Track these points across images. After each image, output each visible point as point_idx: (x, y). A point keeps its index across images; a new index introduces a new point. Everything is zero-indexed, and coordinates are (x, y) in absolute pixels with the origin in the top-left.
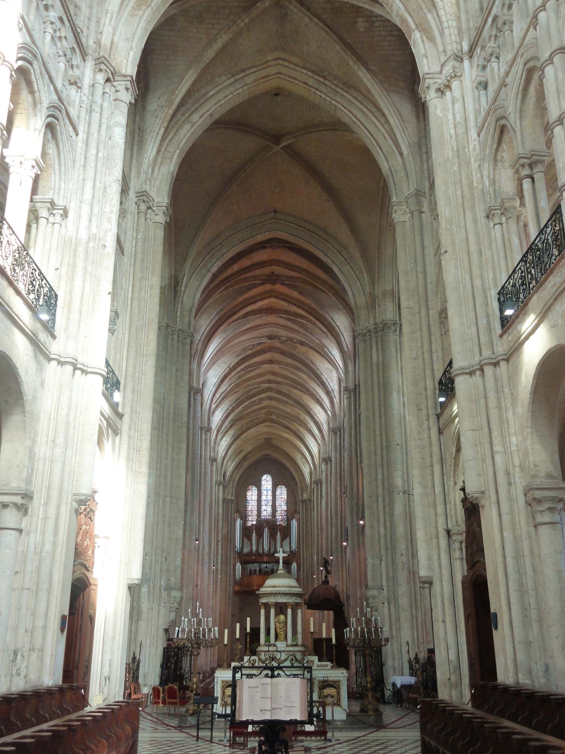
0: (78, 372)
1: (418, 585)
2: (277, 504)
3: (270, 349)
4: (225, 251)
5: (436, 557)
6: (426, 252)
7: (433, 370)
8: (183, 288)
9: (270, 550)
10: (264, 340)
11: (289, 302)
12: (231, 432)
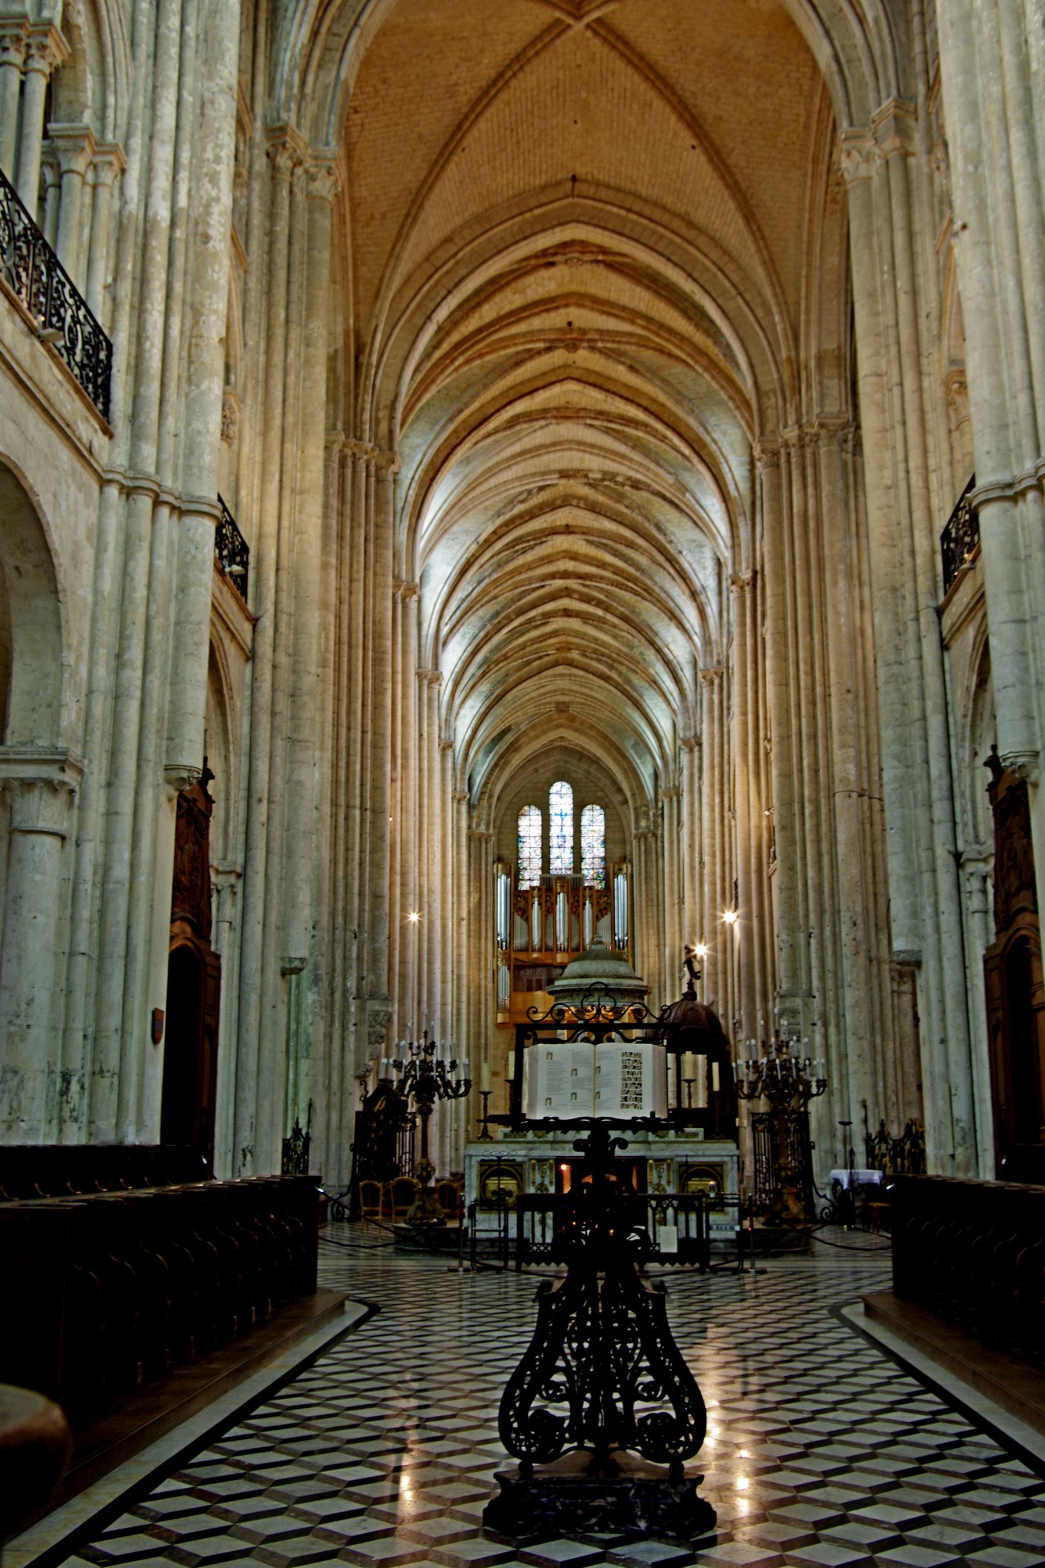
0: (164, 511)
1: (888, 986)
2: (584, 844)
3: (567, 501)
4: (464, 272)
5: (929, 910)
6: (918, 248)
7: (929, 510)
8: (374, 359)
9: (569, 939)
10: (553, 479)
11: (608, 391)
12: (484, 687)
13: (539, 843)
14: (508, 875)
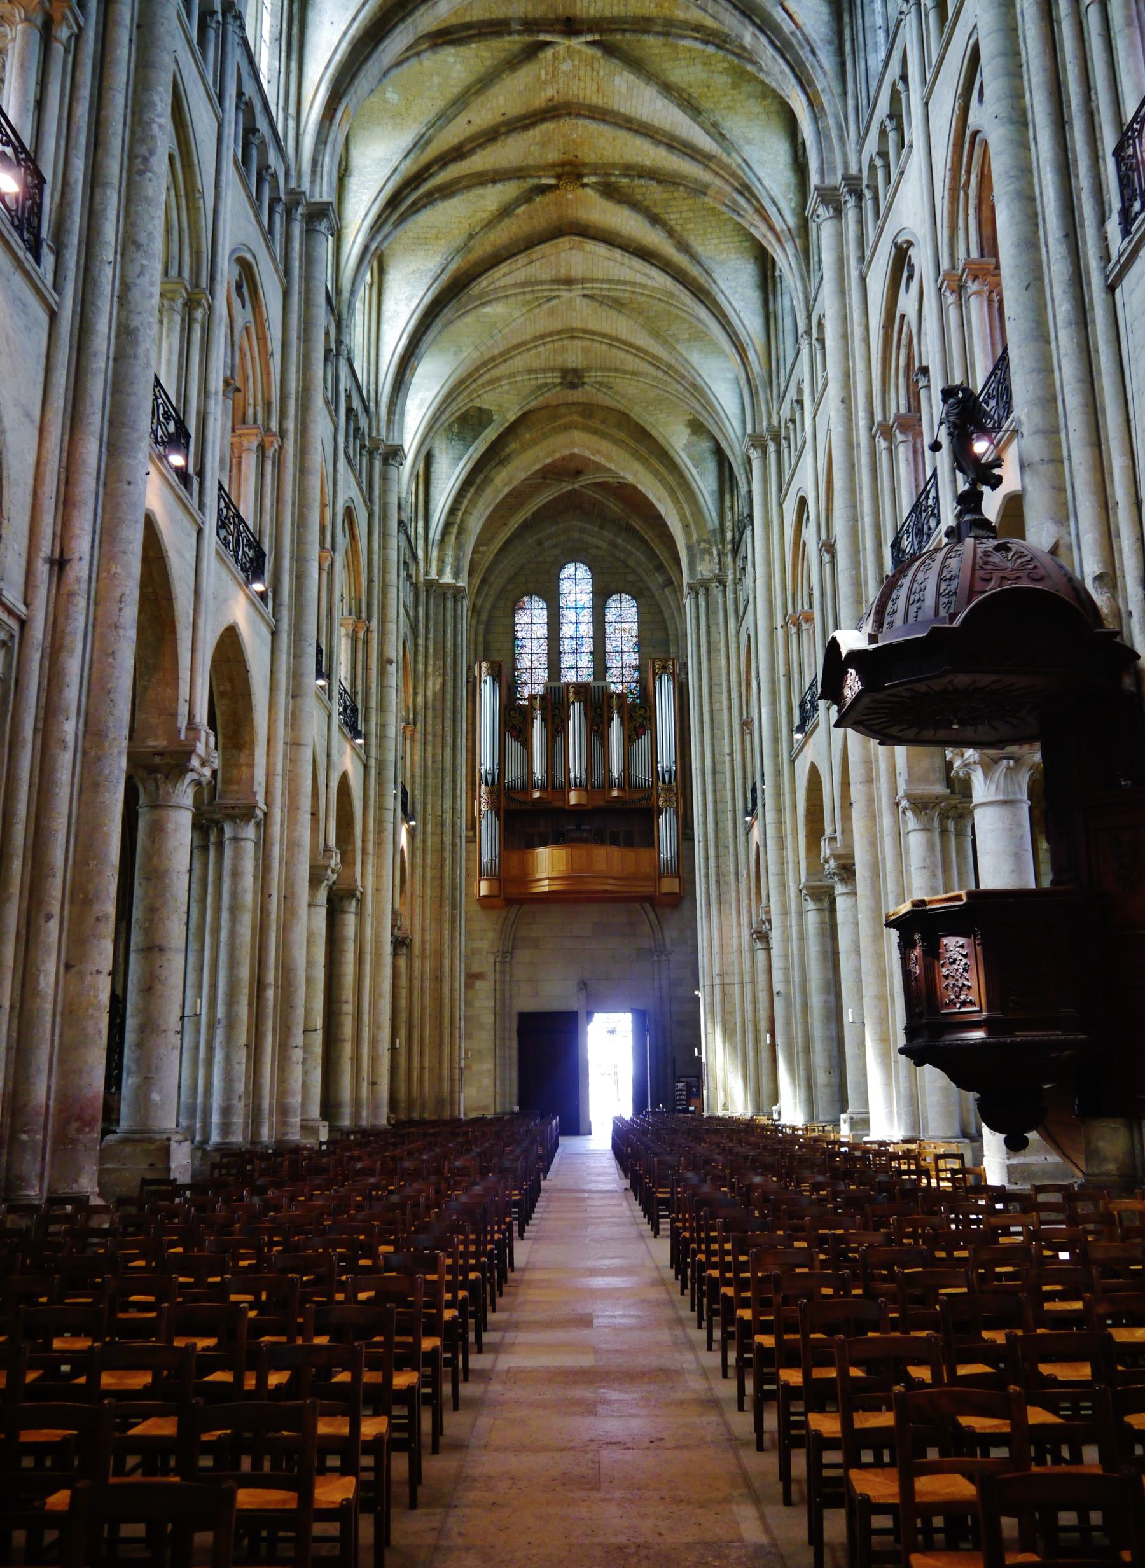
2: (608, 648)
9: (589, 771)
13: (545, 647)
14: (496, 674)
